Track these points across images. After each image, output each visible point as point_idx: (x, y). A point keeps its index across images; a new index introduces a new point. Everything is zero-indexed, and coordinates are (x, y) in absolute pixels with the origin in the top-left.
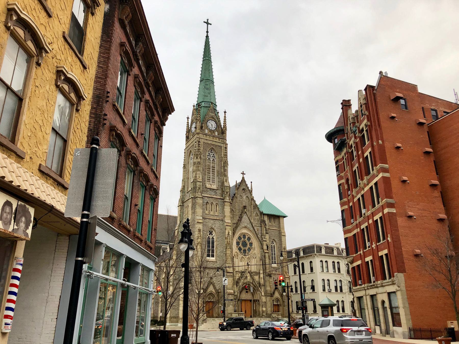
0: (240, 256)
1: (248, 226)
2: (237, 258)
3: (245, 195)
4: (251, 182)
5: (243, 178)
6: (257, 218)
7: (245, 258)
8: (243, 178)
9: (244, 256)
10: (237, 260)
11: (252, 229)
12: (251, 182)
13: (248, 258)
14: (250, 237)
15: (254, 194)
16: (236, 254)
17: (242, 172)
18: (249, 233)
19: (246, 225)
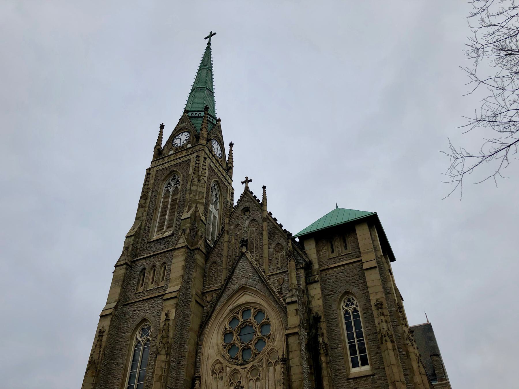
0: (228, 369)
1: (250, 282)
2: (222, 378)
3: (247, 219)
4: (264, 187)
5: (247, 188)
6: (280, 255)
7: (240, 370)
8: (247, 188)
9: (239, 368)
10: (221, 383)
11: (259, 286)
12: (264, 187)
13: (253, 369)
14: (262, 308)
15: (270, 208)
16: (218, 366)
17: (249, 179)
18: (262, 302)
19: (243, 282)
